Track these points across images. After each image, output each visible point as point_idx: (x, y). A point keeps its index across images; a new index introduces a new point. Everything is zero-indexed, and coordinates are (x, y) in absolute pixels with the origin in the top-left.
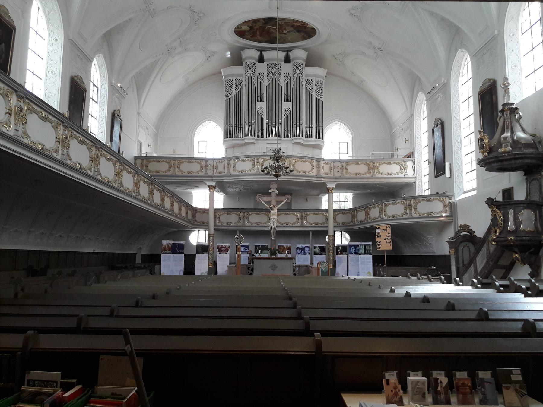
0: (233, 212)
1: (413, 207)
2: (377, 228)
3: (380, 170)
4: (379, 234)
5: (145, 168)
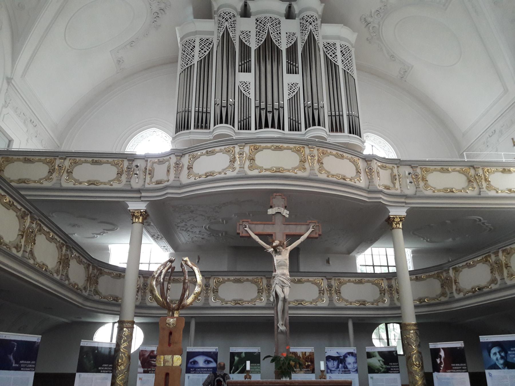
3: (492, 183)
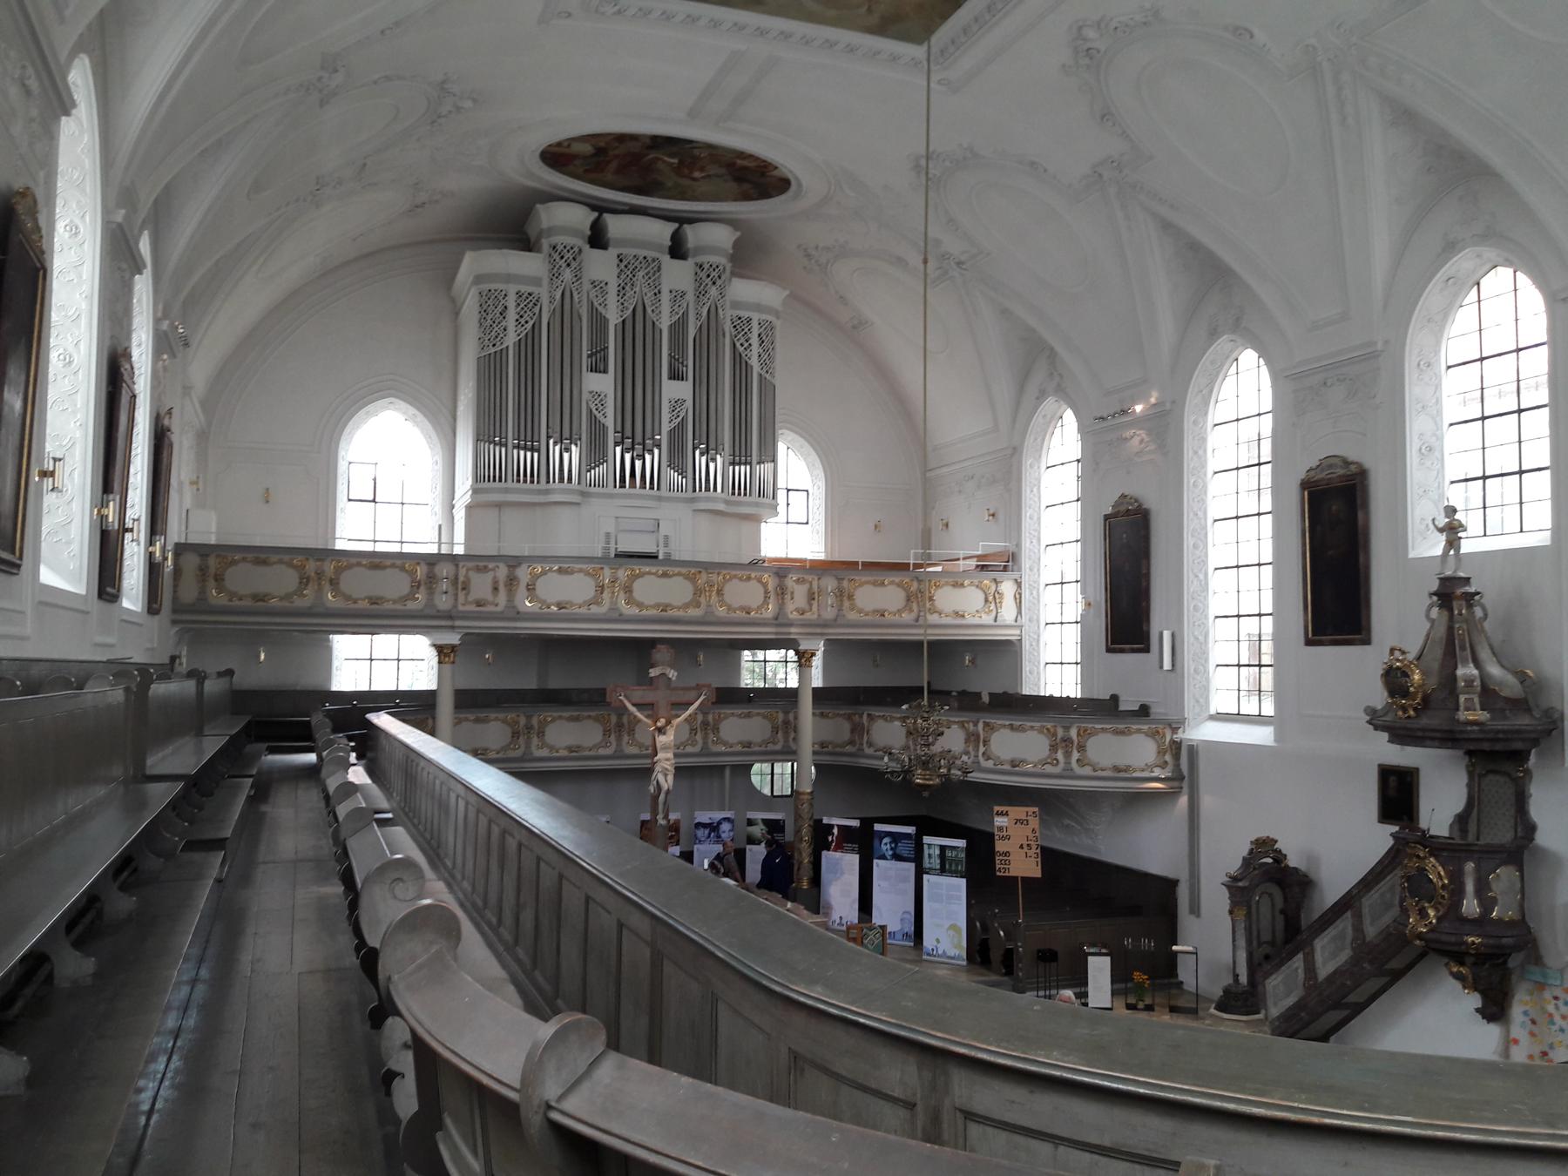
0: (493, 716)
1: (1076, 744)
2: (998, 814)
4: (1005, 829)
5: (211, 583)
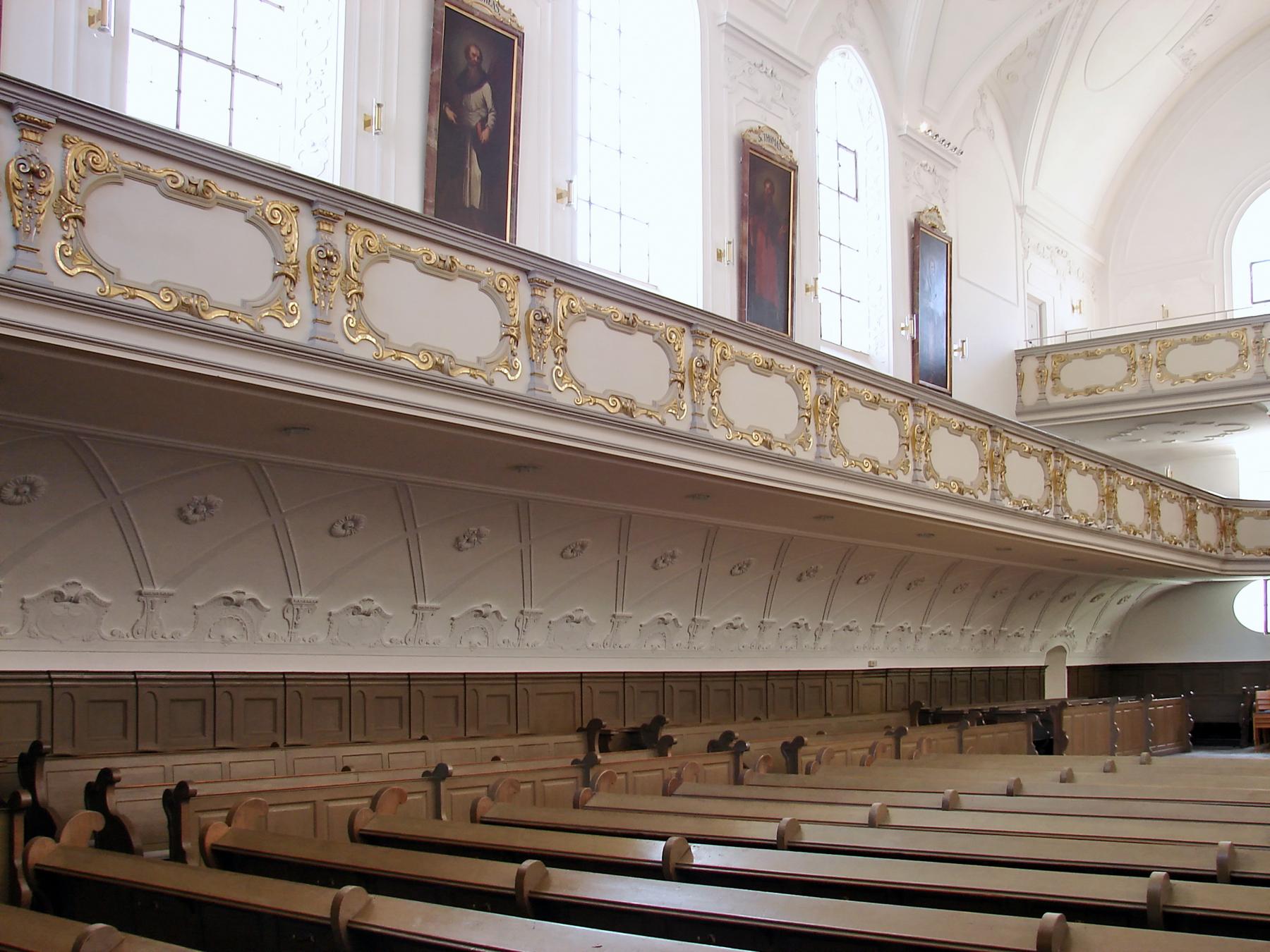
5: (1050, 384)
